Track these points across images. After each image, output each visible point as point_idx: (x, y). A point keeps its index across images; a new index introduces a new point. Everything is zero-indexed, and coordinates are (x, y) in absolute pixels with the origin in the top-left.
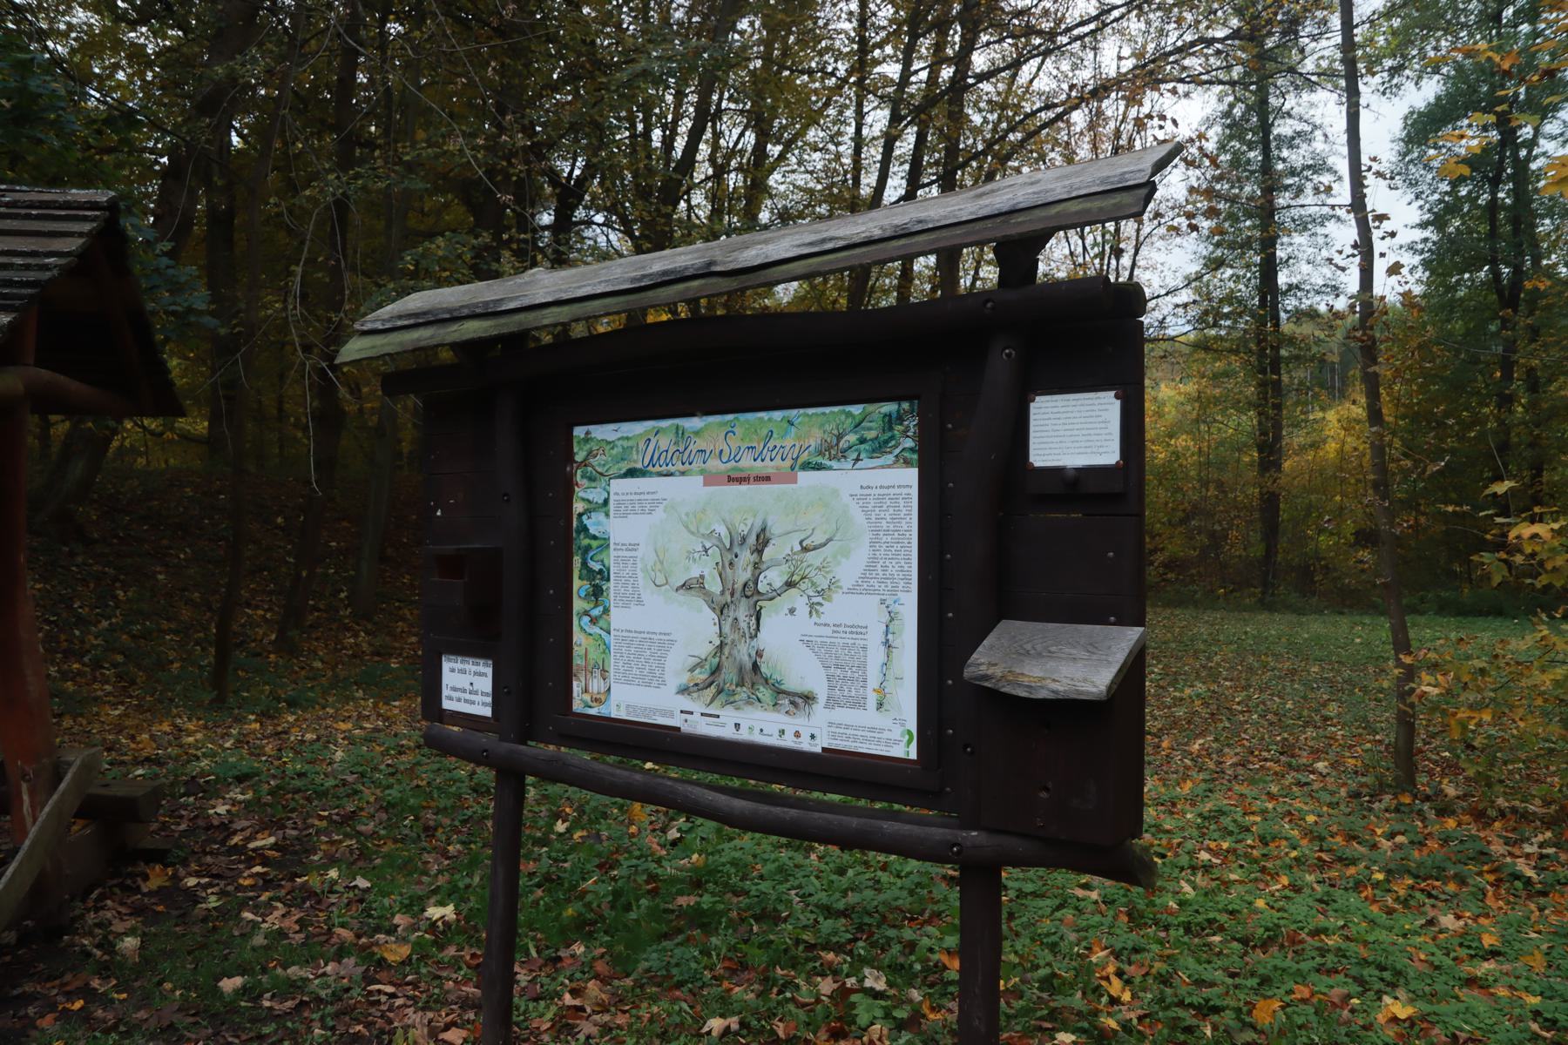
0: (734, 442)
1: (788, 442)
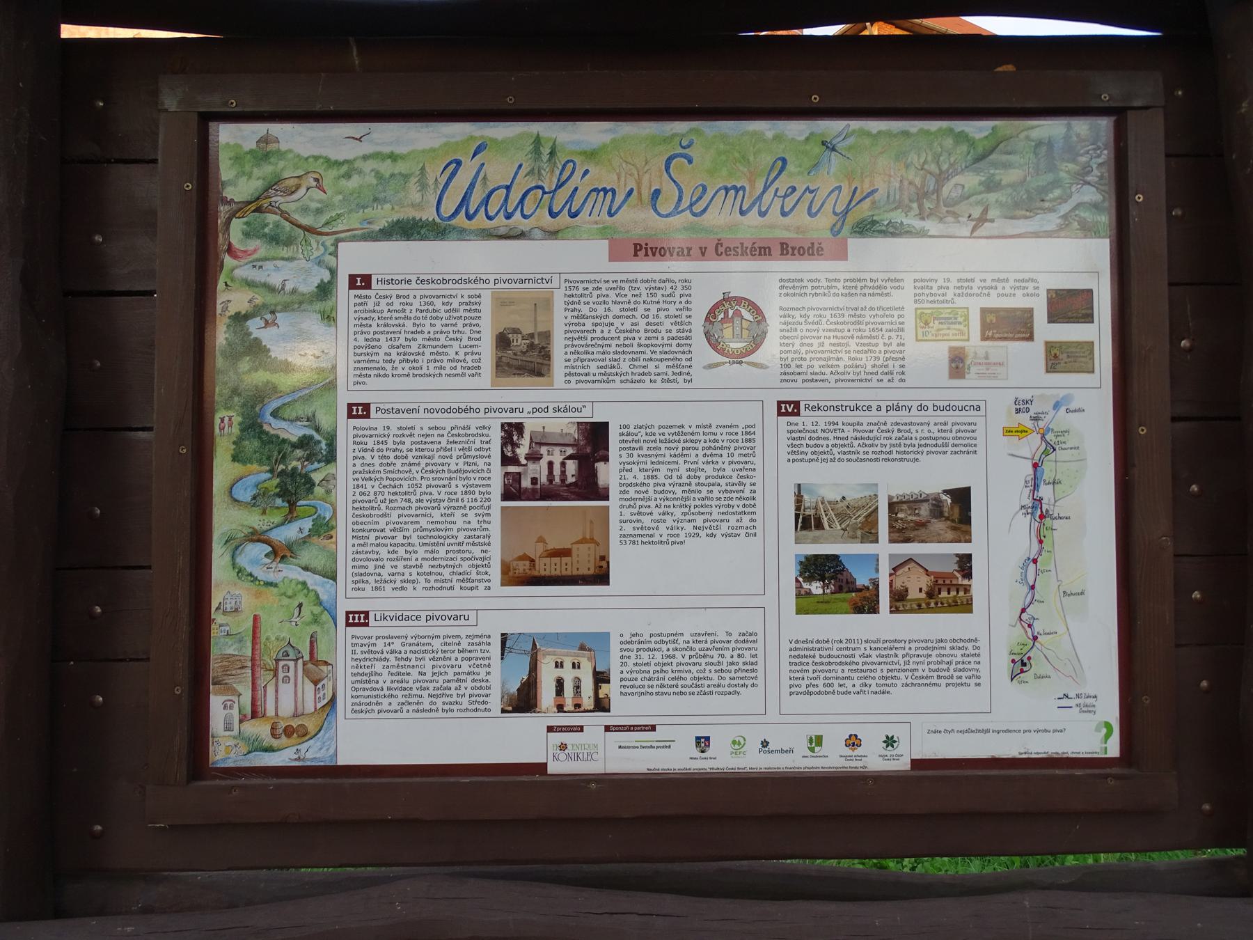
0: (689, 179)
1: (825, 181)
